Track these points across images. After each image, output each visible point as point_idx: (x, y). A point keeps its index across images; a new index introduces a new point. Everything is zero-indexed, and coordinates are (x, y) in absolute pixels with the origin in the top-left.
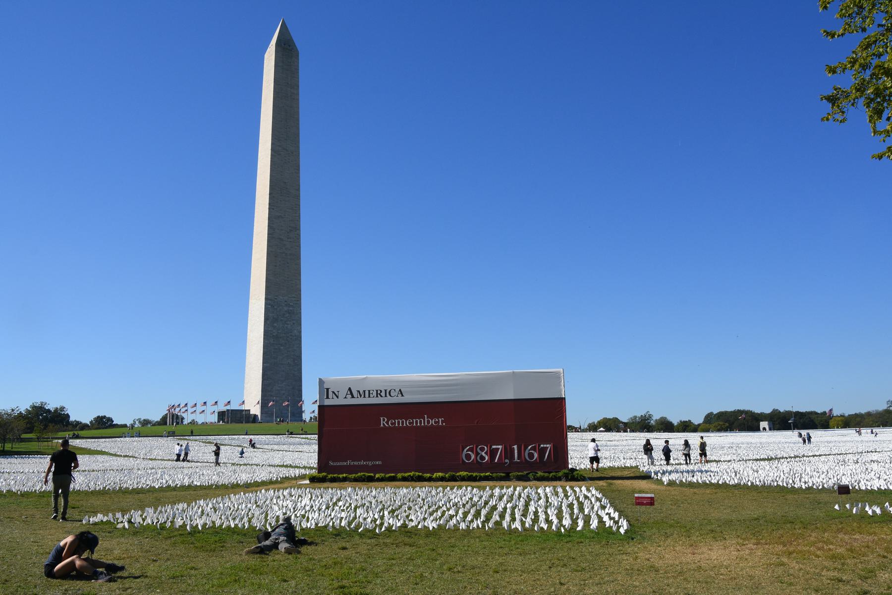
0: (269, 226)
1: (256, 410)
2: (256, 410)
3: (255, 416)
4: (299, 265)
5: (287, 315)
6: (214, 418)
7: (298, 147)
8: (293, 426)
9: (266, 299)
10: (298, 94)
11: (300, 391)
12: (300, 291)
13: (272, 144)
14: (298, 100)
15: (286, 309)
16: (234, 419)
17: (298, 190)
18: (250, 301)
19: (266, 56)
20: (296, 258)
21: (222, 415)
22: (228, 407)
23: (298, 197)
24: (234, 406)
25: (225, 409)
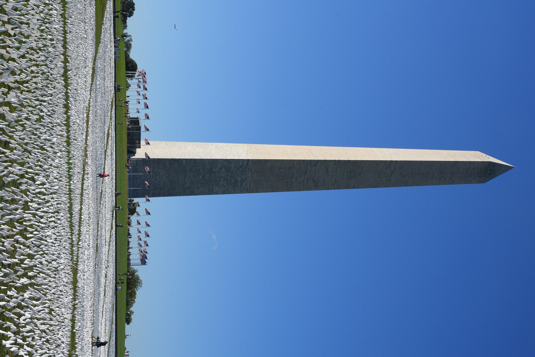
0: (318, 161)
1: (140, 154)
2: (140, 154)
3: (134, 153)
4: (282, 190)
5: (233, 181)
6: (132, 114)
7: (394, 186)
8: (125, 189)
9: (248, 160)
10: (445, 184)
11: (159, 195)
12: (256, 192)
13: (397, 161)
14: (440, 184)
15: (239, 179)
16: (130, 134)
17: (354, 187)
18: (245, 145)
19: (478, 153)
20: (288, 187)
21: (135, 122)
22: (143, 129)
23: (347, 187)
24: (144, 135)
25: (143, 123)
